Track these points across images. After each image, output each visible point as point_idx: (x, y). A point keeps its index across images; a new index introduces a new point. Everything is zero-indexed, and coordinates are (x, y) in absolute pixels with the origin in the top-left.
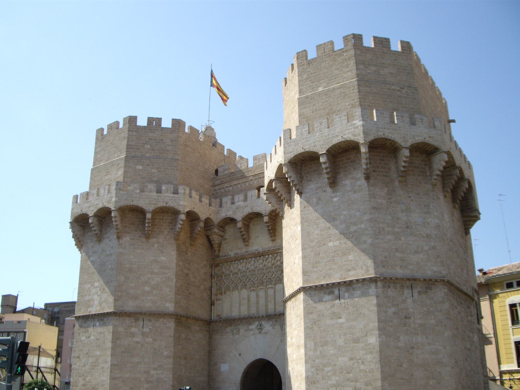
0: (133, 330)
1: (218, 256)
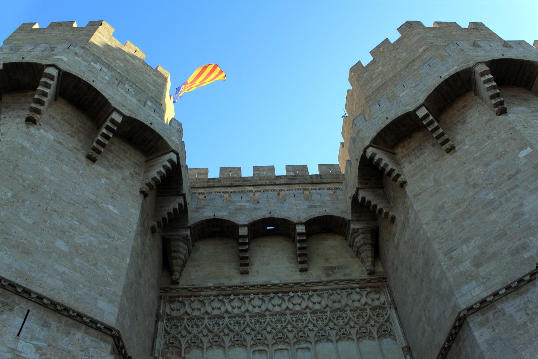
1: (176, 283)
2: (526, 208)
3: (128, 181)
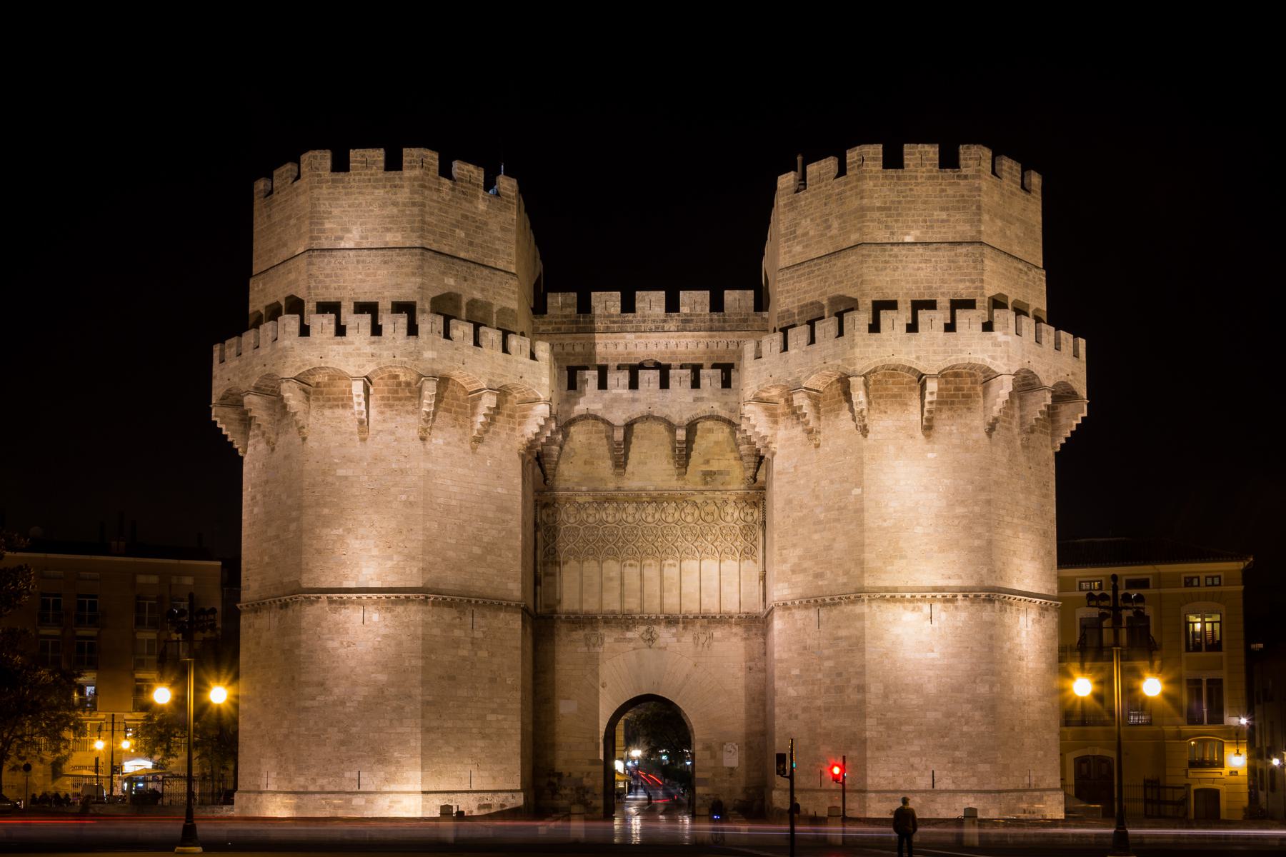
0: (458, 633)
2: (836, 545)
3: (508, 446)
